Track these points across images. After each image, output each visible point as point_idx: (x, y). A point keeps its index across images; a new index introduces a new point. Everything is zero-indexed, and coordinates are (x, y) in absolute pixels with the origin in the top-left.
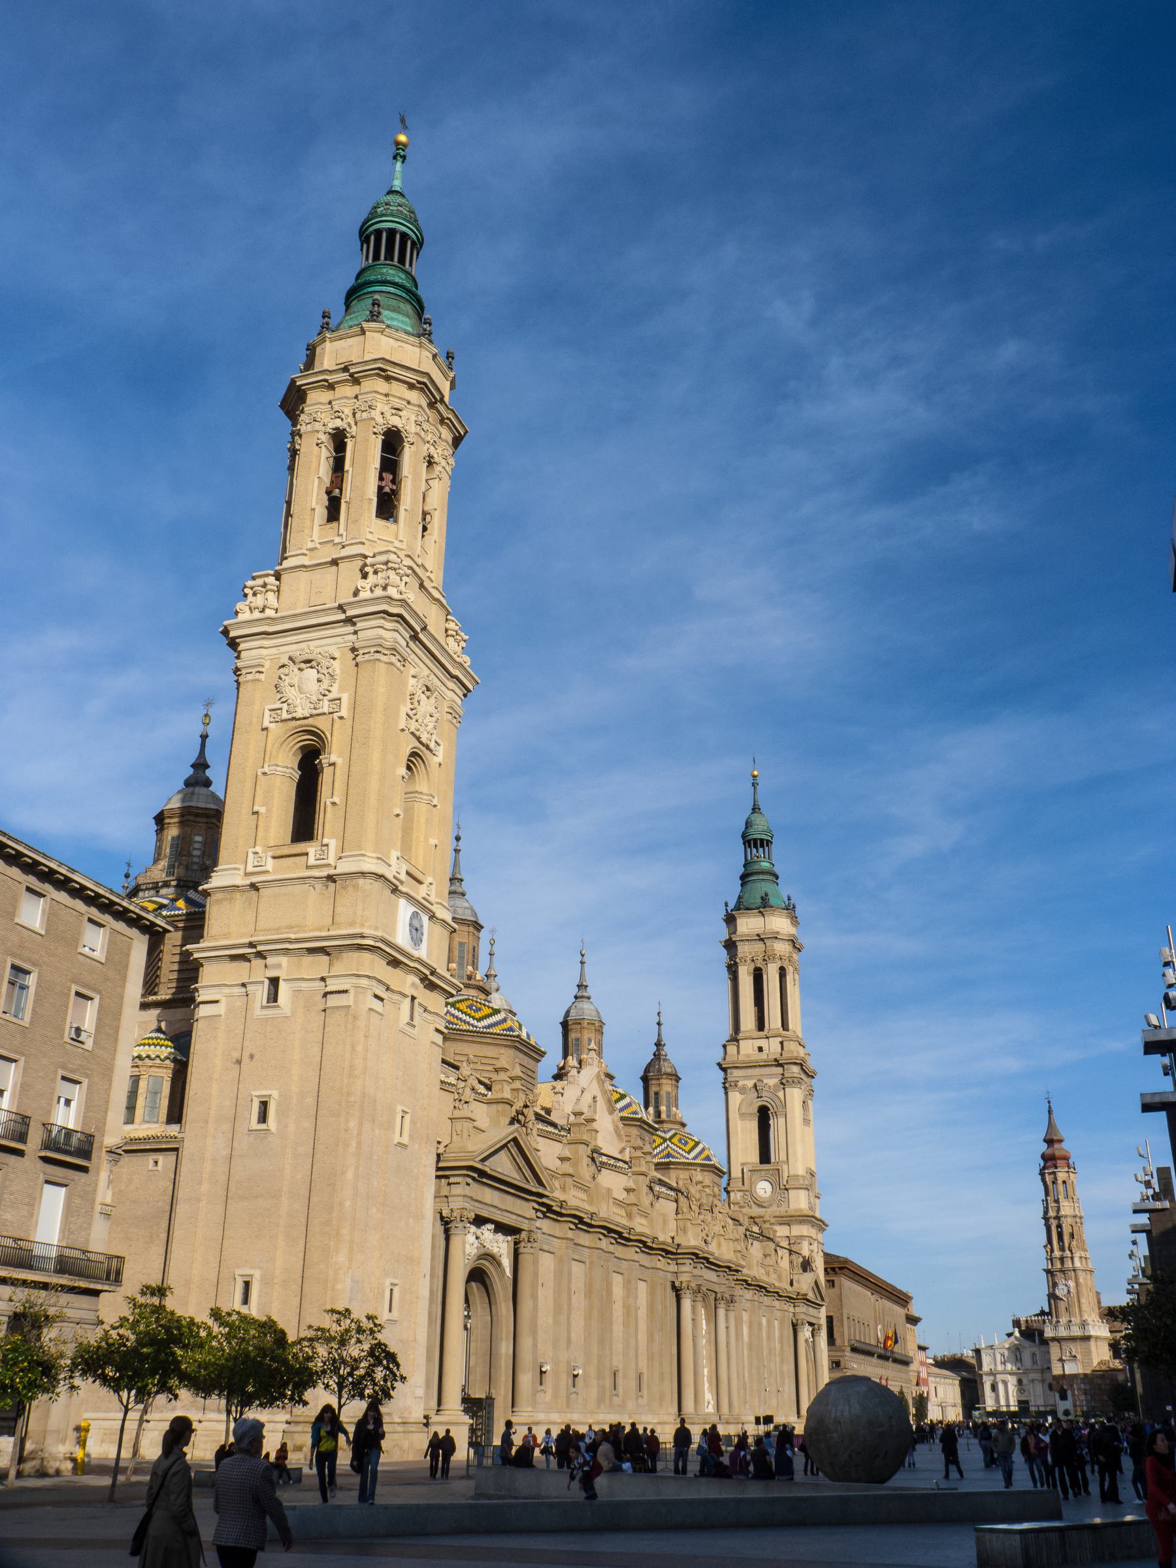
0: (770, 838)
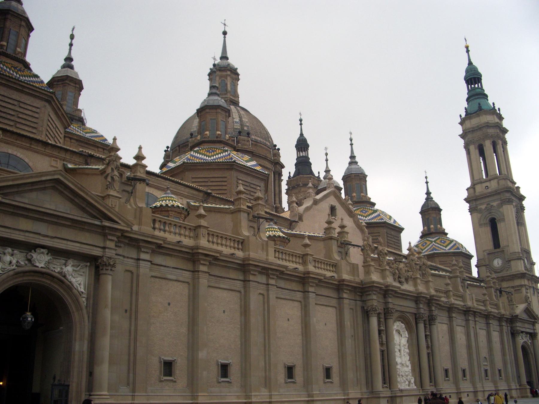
0: (480, 77)
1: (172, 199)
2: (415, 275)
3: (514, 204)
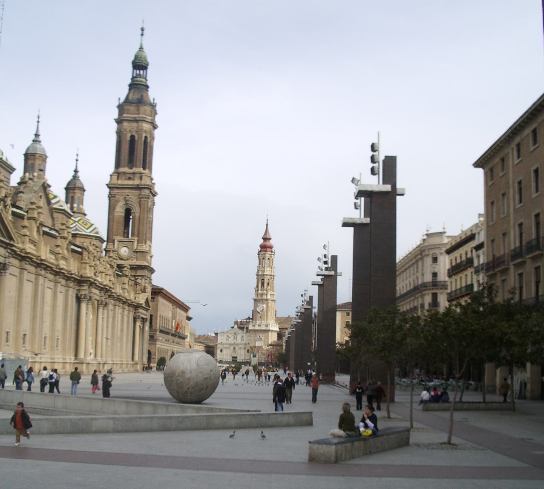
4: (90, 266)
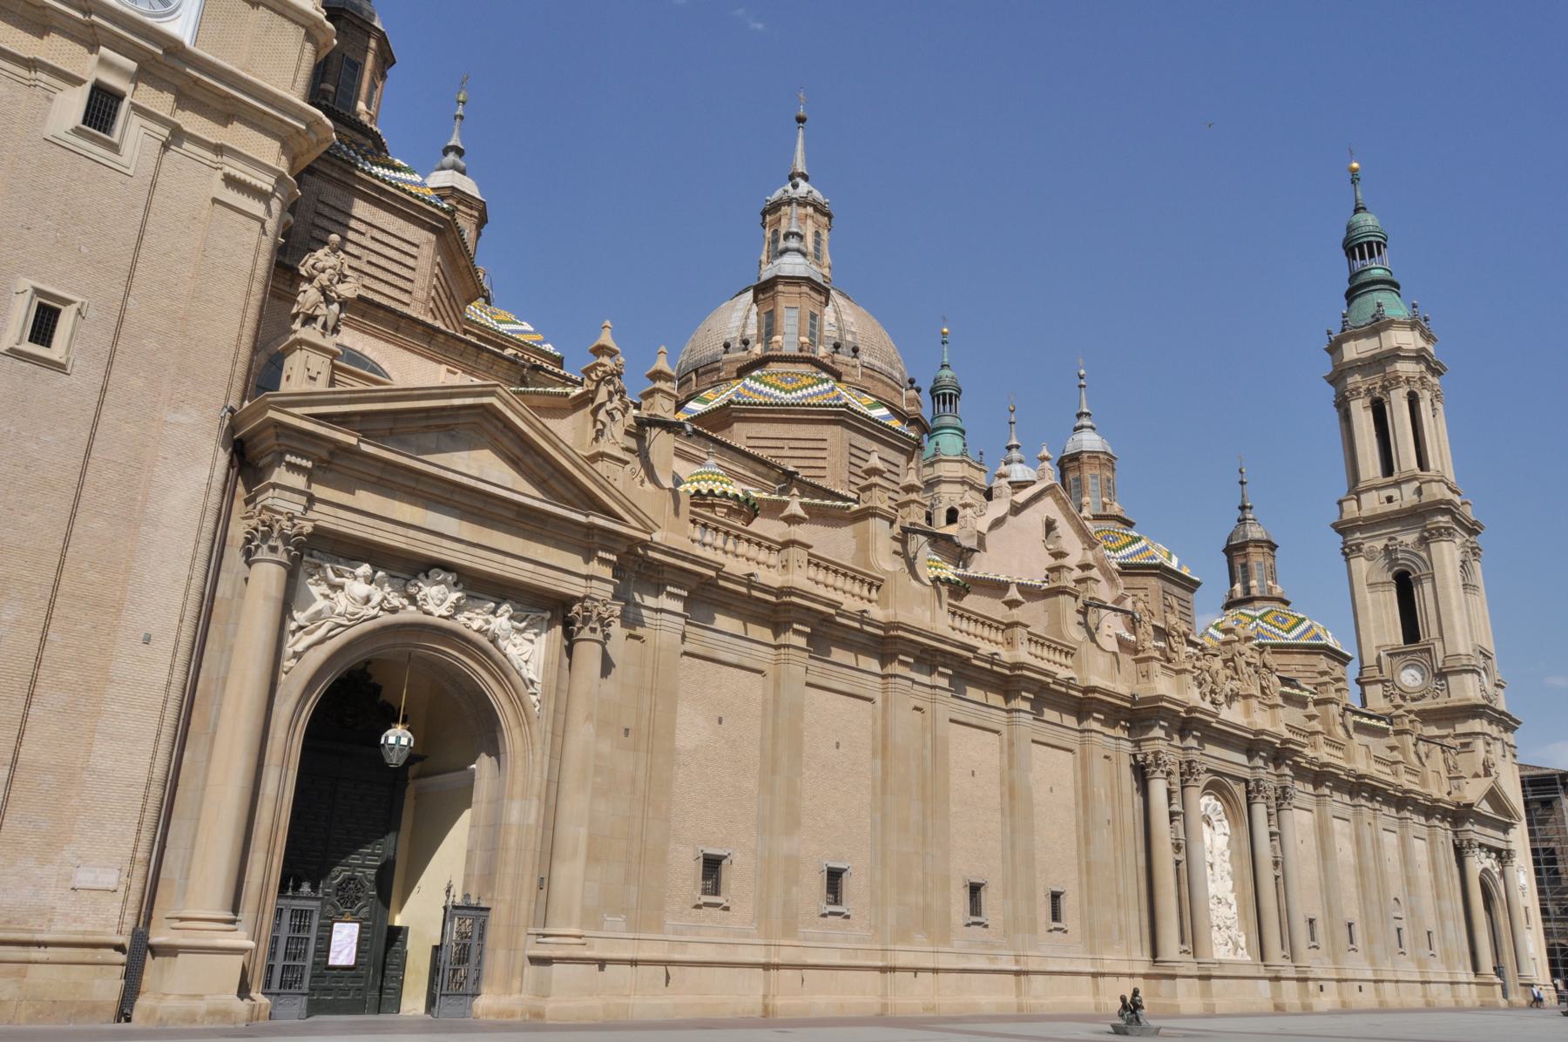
0: (1381, 240)
1: (721, 478)
2: (1246, 690)
3: (1457, 540)
4: (1179, 672)
